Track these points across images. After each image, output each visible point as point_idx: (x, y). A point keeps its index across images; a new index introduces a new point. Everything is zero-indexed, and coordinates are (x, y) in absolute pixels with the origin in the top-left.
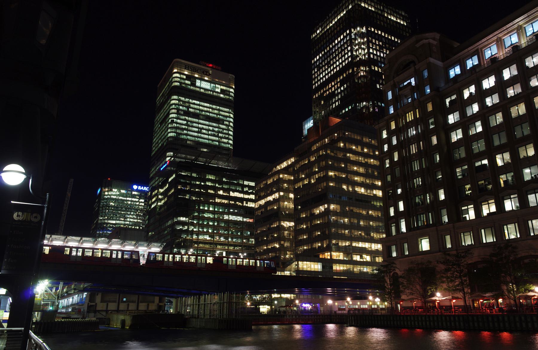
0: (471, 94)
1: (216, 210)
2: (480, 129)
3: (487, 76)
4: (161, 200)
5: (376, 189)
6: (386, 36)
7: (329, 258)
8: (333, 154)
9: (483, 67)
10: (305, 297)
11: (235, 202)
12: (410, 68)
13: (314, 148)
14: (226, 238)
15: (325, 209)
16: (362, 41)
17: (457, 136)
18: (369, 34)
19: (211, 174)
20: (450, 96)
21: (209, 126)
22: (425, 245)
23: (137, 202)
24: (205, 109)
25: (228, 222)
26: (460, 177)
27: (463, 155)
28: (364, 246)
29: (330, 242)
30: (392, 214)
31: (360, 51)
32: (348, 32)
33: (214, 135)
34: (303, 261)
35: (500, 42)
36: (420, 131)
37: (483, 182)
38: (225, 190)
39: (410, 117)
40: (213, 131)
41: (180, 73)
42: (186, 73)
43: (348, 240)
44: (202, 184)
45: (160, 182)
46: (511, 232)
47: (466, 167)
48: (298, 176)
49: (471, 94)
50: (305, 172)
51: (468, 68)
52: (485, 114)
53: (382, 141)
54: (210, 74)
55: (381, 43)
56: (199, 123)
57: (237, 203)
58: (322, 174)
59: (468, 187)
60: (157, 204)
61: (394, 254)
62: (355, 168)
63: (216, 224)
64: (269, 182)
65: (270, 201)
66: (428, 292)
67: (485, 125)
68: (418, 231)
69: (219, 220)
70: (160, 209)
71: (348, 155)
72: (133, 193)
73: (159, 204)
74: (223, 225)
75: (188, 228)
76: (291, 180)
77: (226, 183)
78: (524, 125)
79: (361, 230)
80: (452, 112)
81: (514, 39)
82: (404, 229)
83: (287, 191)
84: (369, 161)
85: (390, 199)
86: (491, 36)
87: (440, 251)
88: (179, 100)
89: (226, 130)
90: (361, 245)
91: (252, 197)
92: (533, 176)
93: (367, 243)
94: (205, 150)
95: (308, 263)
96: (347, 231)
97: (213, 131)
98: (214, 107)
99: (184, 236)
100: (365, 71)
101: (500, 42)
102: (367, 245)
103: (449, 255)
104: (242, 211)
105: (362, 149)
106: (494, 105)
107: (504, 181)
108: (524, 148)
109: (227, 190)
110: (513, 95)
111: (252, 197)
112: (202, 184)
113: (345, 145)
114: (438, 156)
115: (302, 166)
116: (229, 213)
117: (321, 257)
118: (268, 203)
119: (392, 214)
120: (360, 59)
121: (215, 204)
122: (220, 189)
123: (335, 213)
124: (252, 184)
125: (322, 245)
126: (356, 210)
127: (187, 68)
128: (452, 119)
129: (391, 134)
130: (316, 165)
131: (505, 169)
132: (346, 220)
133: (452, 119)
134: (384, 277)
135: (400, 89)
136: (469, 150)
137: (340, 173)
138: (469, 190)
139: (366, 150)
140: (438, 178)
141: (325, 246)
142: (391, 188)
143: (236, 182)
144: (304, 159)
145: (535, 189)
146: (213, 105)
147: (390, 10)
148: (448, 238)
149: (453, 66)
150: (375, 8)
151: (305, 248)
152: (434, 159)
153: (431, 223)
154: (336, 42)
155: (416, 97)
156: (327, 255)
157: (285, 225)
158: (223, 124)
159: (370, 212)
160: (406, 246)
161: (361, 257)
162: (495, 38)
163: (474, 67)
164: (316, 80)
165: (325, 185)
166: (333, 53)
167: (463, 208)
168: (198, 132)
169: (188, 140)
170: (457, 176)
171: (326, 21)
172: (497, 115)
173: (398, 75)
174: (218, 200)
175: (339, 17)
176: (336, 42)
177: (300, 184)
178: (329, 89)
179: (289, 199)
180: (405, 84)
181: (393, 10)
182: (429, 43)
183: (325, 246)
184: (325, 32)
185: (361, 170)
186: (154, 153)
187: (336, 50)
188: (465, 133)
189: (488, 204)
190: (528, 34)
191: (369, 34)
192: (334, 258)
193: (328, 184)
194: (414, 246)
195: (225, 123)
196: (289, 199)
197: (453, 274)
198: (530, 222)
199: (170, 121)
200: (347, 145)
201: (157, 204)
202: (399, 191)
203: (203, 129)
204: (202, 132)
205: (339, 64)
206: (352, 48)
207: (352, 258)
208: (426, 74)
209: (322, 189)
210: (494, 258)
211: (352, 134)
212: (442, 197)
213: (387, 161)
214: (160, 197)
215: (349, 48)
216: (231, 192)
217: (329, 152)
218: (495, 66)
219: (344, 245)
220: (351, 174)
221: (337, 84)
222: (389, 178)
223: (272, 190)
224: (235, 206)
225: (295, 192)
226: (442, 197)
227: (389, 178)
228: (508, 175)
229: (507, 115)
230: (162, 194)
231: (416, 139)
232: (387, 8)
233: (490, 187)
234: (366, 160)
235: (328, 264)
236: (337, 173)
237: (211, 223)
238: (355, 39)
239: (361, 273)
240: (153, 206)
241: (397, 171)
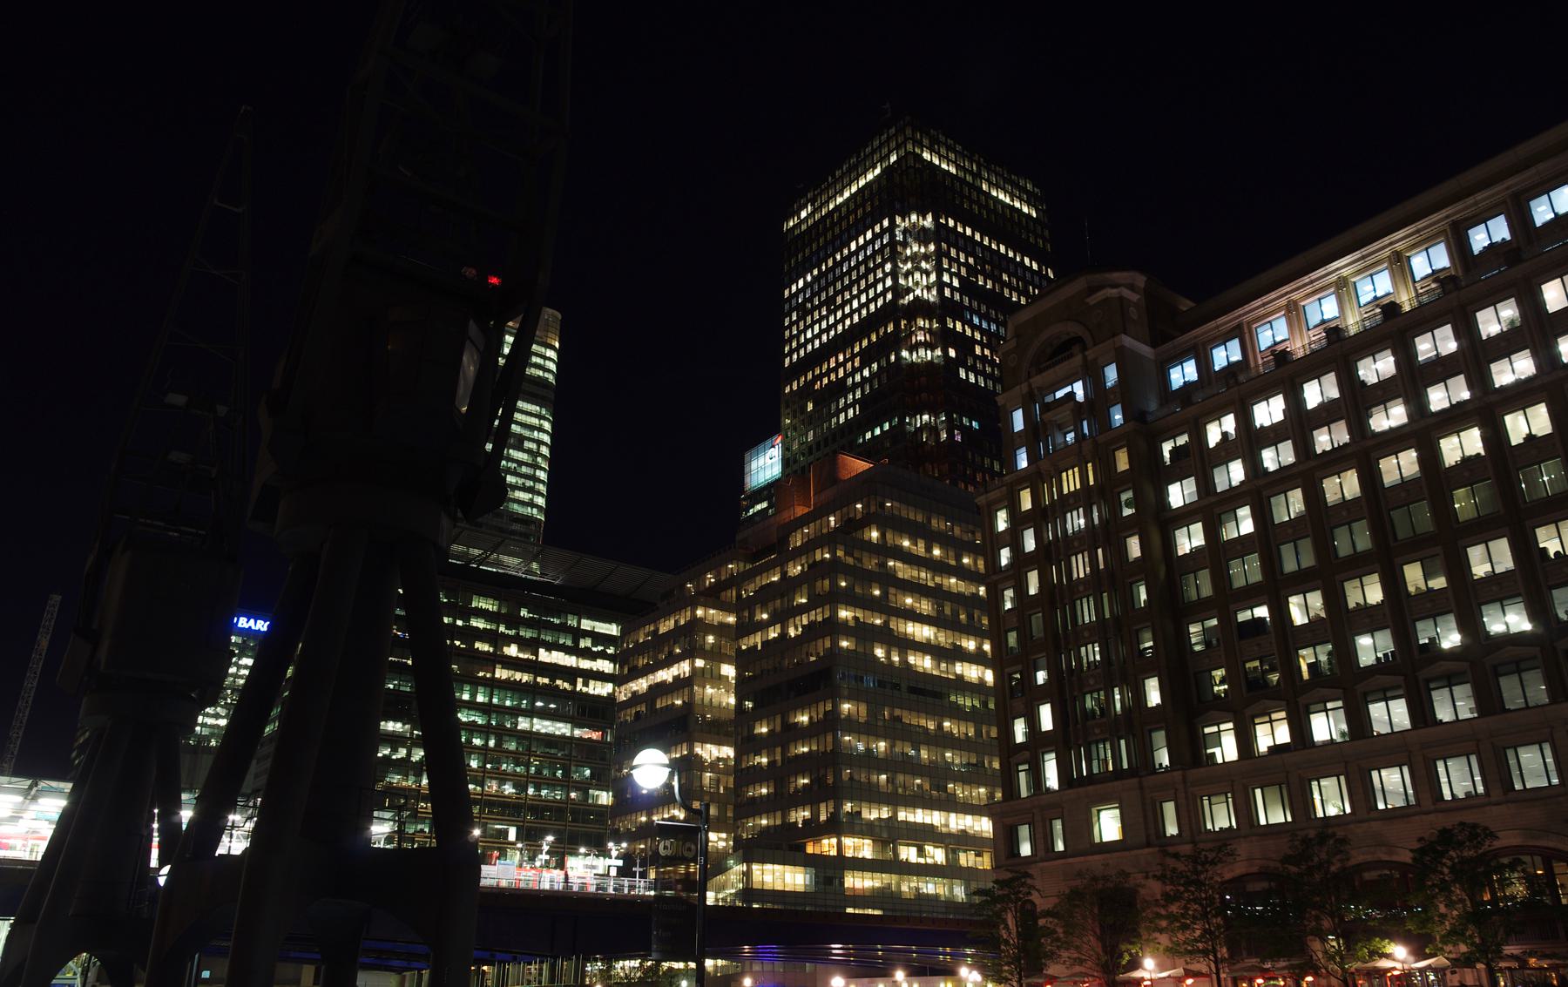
0: (1225, 435)
1: (495, 701)
2: (1247, 526)
3: (1265, 395)
5: (962, 661)
6: (986, 242)
7: (834, 852)
8: (850, 560)
9: (1253, 374)
10: (768, 967)
11: (553, 680)
12: (1072, 356)
13: (797, 540)
14: (521, 787)
15: (826, 713)
16: (923, 250)
17: (1190, 539)
18: (940, 234)
19: (485, 595)
20: (1174, 437)
22: (1109, 826)
25: (529, 736)
26: (1198, 648)
27: (1207, 591)
28: (928, 820)
29: (838, 807)
30: (1020, 737)
31: (917, 275)
32: (886, 223)
34: (763, 862)
35: (1294, 312)
36: (1096, 521)
37: (1257, 663)
38: (523, 644)
39: (1071, 482)
43: (888, 804)
44: (459, 623)
46: (1330, 799)
47: (1214, 622)
48: (752, 615)
49: (1225, 435)
50: (771, 606)
51: (1217, 368)
52: (1260, 490)
53: (995, 542)
55: (971, 260)
57: (559, 682)
58: (818, 616)
59: (1219, 674)
61: (1026, 850)
62: (909, 601)
63: (492, 743)
64: (663, 630)
65: (663, 683)
66: (1121, 956)
67: (1262, 516)
68: (1090, 788)
69: (501, 733)
71: (891, 563)
74: (512, 746)
75: (409, 754)
76: (728, 625)
77: (528, 623)
78: (1355, 526)
79: (921, 776)
80: (1180, 478)
81: (1330, 308)
82: (1052, 779)
83: (716, 656)
84: (945, 582)
85: (1014, 696)
86: (1273, 295)
87: (1148, 845)
89: (527, 464)
90: (920, 816)
91: (606, 666)
92: (1380, 655)
93: (936, 813)
95: (777, 867)
96: (884, 777)
99: (395, 779)
100: (930, 331)
101: (1294, 312)
102: (935, 818)
103: (1176, 856)
104: (570, 708)
105: (929, 549)
106: (1282, 469)
107: (1309, 666)
108: (1357, 582)
109: (532, 645)
110: (1329, 448)
111: (606, 666)
112: (459, 623)
113: (883, 535)
114: (1143, 590)
115: (762, 587)
116: (531, 713)
117: (810, 849)
118: (660, 689)
119: (1020, 737)
120: (917, 298)
121: (493, 685)
122: (509, 640)
123: (851, 725)
124: (613, 629)
125: (815, 814)
126: (911, 719)
128: (1179, 494)
129: (1019, 521)
130: (805, 588)
131: (1313, 633)
132: (882, 745)
133: (1179, 494)
134: (998, 915)
135: (1046, 408)
136: (1221, 578)
137: (868, 613)
138: (1222, 682)
139: (937, 552)
140: (1138, 648)
141: (823, 818)
142: (1020, 667)
143: (557, 621)
144: (768, 568)
145: (1385, 690)
148: (1169, 809)
149: (1179, 359)
150: (958, 167)
151: (764, 822)
152: (1132, 597)
153: (1125, 766)
154: (853, 246)
155: (1086, 431)
156: (828, 846)
157: (706, 756)
158: (524, 451)
159: (947, 724)
160: (1058, 825)
161: (921, 852)
162: (1283, 301)
163: (1231, 368)
164: (794, 345)
165: (828, 644)
166: (843, 275)
167: (1207, 730)
170: (1191, 645)
171: (827, 189)
172: (1290, 494)
173: (1040, 371)
174: (501, 674)
175: (862, 183)
176: (853, 246)
177: (757, 640)
178: (829, 371)
179: (719, 680)
180: (1060, 394)
182: (1121, 298)
183: (823, 818)
184: (823, 218)
185: (925, 607)
187: (851, 269)
188: (1212, 533)
189: (1271, 721)
190: (1363, 300)
191: (940, 234)
192: (849, 854)
193: (835, 643)
194: (1081, 829)
196: (719, 680)
197: (1186, 908)
198: (1375, 774)
200: (889, 536)
202: (1041, 677)
205: (858, 305)
206: (895, 266)
207: (896, 854)
208: (1111, 374)
209: (818, 655)
210: (1293, 869)
211: (903, 507)
212: (1154, 697)
213: (1009, 593)
215: (888, 267)
216: (542, 651)
217: (840, 553)
218: (1285, 373)
219: (874, 815)
220: (898, 616)
222: (1012, 639)
223: (671, 652)
224: (550, 693)
225: (743, 660)
226: (1154, 697)
227: (1012, 639)
228: (1318, 648)
229: (1314, 497)
231: (1087, 540)
233: (1275, 677)
234: (938, 579)
235: (830, 870)
236: (859, 614)
237: (477, 742)
238: (905, 244)
239: (921, 898)
241: (1037, 621)
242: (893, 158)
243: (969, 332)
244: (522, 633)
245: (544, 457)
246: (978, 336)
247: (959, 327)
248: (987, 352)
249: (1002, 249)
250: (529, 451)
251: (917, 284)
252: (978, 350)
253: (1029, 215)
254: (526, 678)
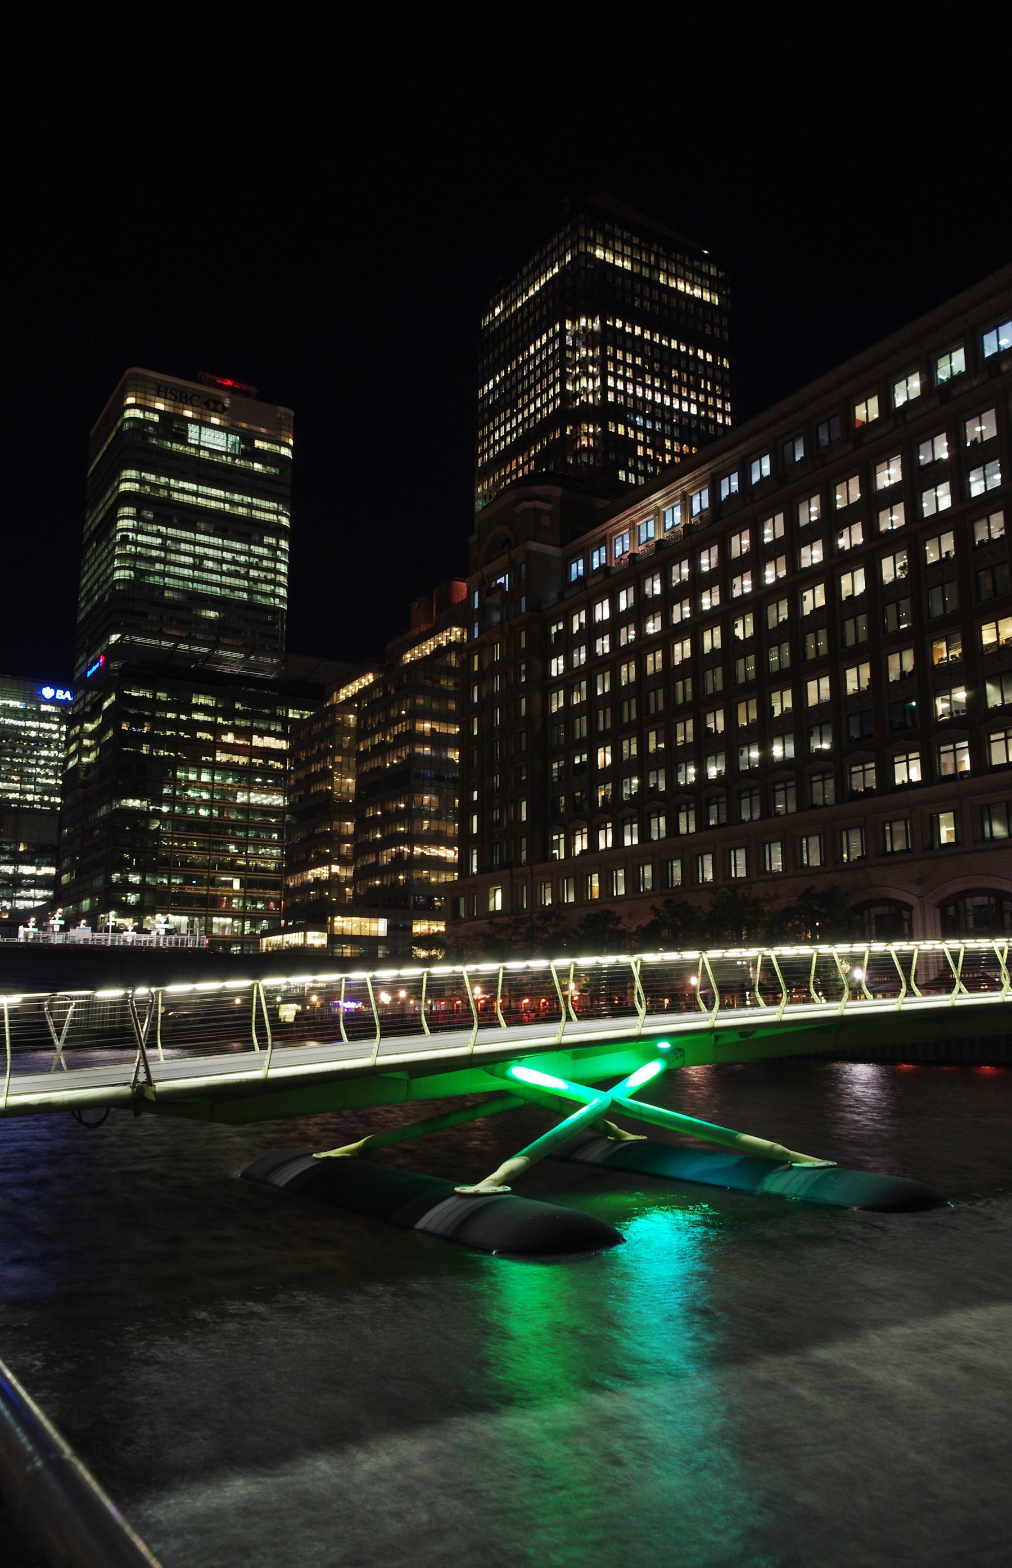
4: (88, 750)
6: (656, 339)
11: (266, 761)
16: (591, 354)
19: (205, 693)
21: (223, 549)
23: (54, 732)
25: (247, 808)
33: (236, 575)
38: (238, 732)
41: (144, 408)
42: (160, 406)
45: (85, 705)
54: (224, 409)
55: (638, 361)
56: (195, 543)
60: (80, 760)
70: (87, 773)
72: (44, 708)
73: (85, 760)
77: (243, 715)
88: (142, 482)
89: (267, 559)
97: (234, 562)
98: (237, 497)
100: (594, 435)
109: (245, 733)
120: (582, 402)
122: (226, 730)
127: (161, 392)
146: (233, 491)
147: (677, 263)
154: (532, 350)
158: (264, 546)
162: (627, 521)
164: (486, 445)
166: (524, 378)
168: (193, 567)
169: (166, 587)
171: (516, 286)
174: (221, 757)
175: (550, 275)
176: (532, 350)
178: (512, 472)
181: (683, 264)
186: (82, 616)
187: (529, 373)
199: (118, 537)
201: (80, 760)
204: (203, 565)
214: (87, 742)
215: (558, 373)
216: (255, 737)
221: (528, 463)
230: (91, 736)
232: (668, 260)
240: (71, 764)
242: (568, 258)
243: (631, 434)
244: (237, 723)
246: (640, 436)
247: (621, 430)
248: (650, 452)
249: (674, 344)
251: (585, 389)
252: (640, 451)
253: (710, 304)
254: (243, 760)
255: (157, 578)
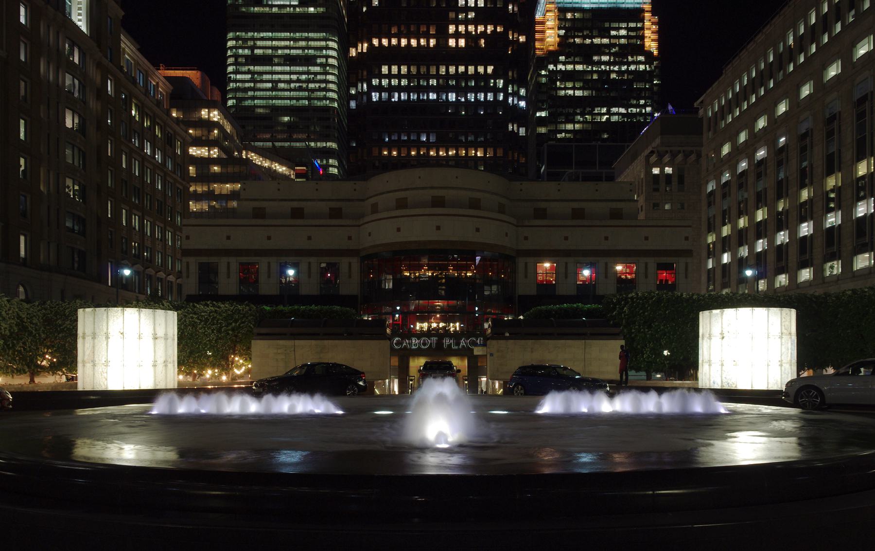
24: (283, 43)
40: (298, 81)
89: (320, 74)
94: (286, 119)
146: (295, 32)
158: (316, 65)
195: (319, 61)
203: (280, 81)
245: (332, 66)
250: (321, 65)
255: (250, 101)
